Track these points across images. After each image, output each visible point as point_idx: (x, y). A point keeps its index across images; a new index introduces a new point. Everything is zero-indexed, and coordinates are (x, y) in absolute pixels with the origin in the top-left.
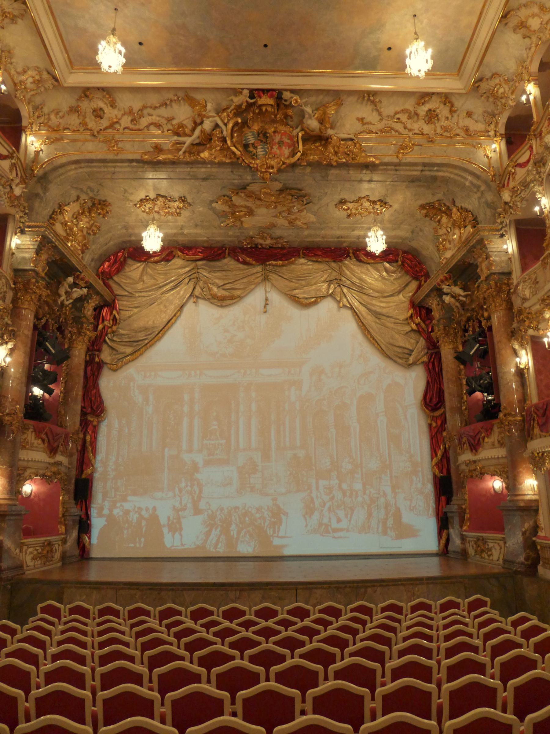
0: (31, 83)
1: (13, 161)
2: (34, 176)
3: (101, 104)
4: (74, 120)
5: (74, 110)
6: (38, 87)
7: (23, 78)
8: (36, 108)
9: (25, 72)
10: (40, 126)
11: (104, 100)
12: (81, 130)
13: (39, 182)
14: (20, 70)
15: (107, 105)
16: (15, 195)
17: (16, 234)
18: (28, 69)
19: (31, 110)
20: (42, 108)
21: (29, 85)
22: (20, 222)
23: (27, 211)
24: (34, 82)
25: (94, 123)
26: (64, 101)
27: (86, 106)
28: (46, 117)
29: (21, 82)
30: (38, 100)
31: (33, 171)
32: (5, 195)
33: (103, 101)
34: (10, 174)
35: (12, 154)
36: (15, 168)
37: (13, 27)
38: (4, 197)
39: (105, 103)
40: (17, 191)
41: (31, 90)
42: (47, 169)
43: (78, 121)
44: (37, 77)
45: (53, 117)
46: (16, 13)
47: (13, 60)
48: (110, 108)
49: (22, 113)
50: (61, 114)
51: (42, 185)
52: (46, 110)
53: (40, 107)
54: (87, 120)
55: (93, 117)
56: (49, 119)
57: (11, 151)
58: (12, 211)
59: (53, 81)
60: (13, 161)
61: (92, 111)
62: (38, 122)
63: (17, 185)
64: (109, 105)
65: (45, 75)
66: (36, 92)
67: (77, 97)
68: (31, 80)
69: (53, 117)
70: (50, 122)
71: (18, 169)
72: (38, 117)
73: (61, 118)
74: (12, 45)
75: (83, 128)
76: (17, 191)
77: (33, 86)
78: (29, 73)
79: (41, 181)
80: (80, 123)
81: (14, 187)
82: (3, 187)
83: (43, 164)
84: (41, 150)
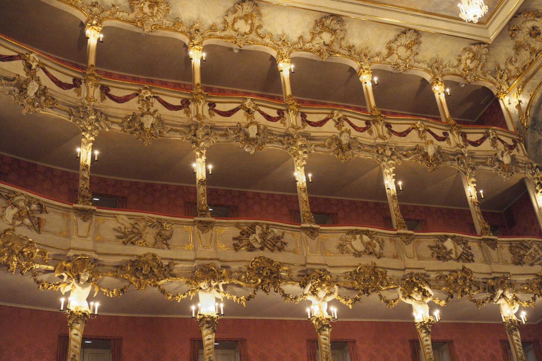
0: (471, 63)
1: (491, 137)
2: (527, 129)
3: (530, 24)
4: (525, 55)
5: (518, 48)
6: (480, 60)
7: (462, 66)
8: (494, 73)
9: (460, 61)
10: (508, 84)
11: (529, 18)
12: (534, 57)
13: (535, 129)
14: (456, 63)
15: (534, 20)
16: (507, 164)
17: (537, 191)
18: (460, 56)
19: (492, 78)
20: (499, 68)
21: (471, 66)
22: (535, 179)
23: (535, 165)
24: (472, 61)
25: (539, 43)
26: (506, 50)
27: (522, 36)
28: (507, 71)
29: (463, 70)
30: (490, 66)
31: (523, 125)
32: (497, 170)
33: (528, 20)
34: (495, 149)
35: (486, 132)
36: (498, 141)
37: (422, 46)
38: (498, 172)
39: (531, 20)
40: (506, 160)
41: (477, 67)
42: (532, 113)
43: (528, 53)
44: (471, 55)
45: (510, 67)
46: (414, 38)
47: (445, 63)
48: (538, 20)
49: (488, 87)
50: (514, 59)
51: (538, 130)
52: (503, 67)
53: (497, 68)
54: (533, 45)
55: (534, 39)
56: (510, 71)
57: (484, 131)
58: (517, 177)
59: (482, 46)
60: (491, 137)
61: (529, 36)
62: (504, 81)
63: (502, 156)
64: (536, 19)
65: (475, 48)
66: (481, 64)
67: (510, 38)
68: (469, 61)
69: (510, 67)
70: (512, 72)
71: (502, 138)
72: (501, 77)
73: (515, 62)
74: (434, 55)
75: (534, 55)
76: (506, 160)
77: (475, 63)
78: (463, 57)
79: (535, 127)
80: (531, 53)
81: (501, 159)
82: (492, 166)
83: (526, 113)
84: (520, 101)
